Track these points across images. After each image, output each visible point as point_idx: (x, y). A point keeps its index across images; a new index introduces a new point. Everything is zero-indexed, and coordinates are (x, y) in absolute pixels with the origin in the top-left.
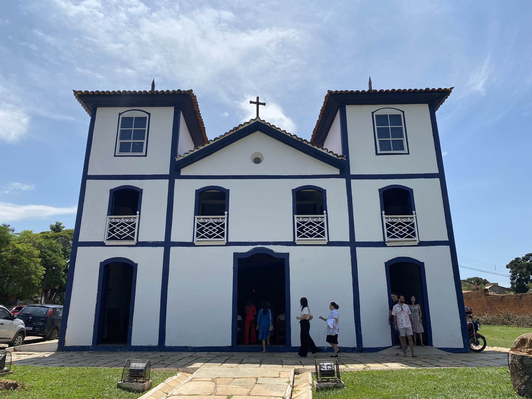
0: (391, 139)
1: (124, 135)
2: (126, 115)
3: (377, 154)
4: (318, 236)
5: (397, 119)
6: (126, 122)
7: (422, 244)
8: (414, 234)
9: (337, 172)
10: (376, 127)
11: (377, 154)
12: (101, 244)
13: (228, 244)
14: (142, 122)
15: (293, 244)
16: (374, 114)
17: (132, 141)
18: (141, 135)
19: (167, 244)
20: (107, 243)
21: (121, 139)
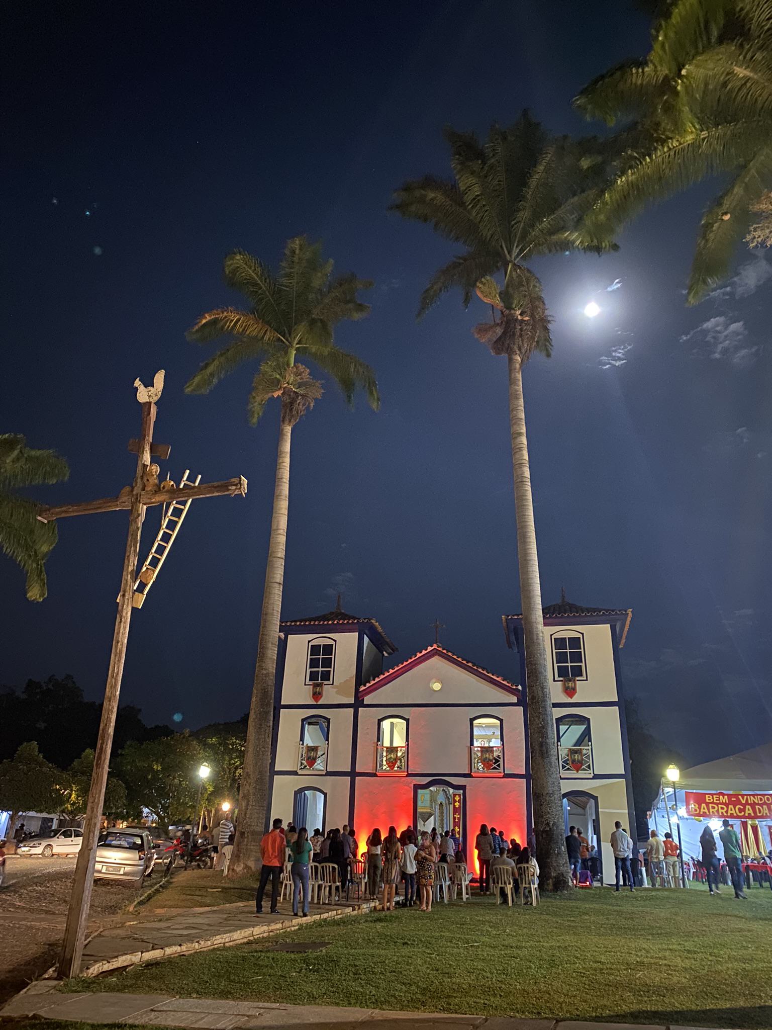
0: (569, 664)
1: (314, 663)
2: (314, 643)
3: (554, 681)
4: (495, 768)
5: (575, 642)
6: (315, 650)
7: (596, 777)
8: (589, 767)
9: (514, 699)
10: (554, 651)
11: (554, 681)
12: (295, 773)
13: (409, 775)
14: (328, 649)
15: (468, 776)
16: (553, 637)
17: (320, 669)
18: (328, 663)
19: (353, 774)
20: (300, 772)
21: (310, 667)
